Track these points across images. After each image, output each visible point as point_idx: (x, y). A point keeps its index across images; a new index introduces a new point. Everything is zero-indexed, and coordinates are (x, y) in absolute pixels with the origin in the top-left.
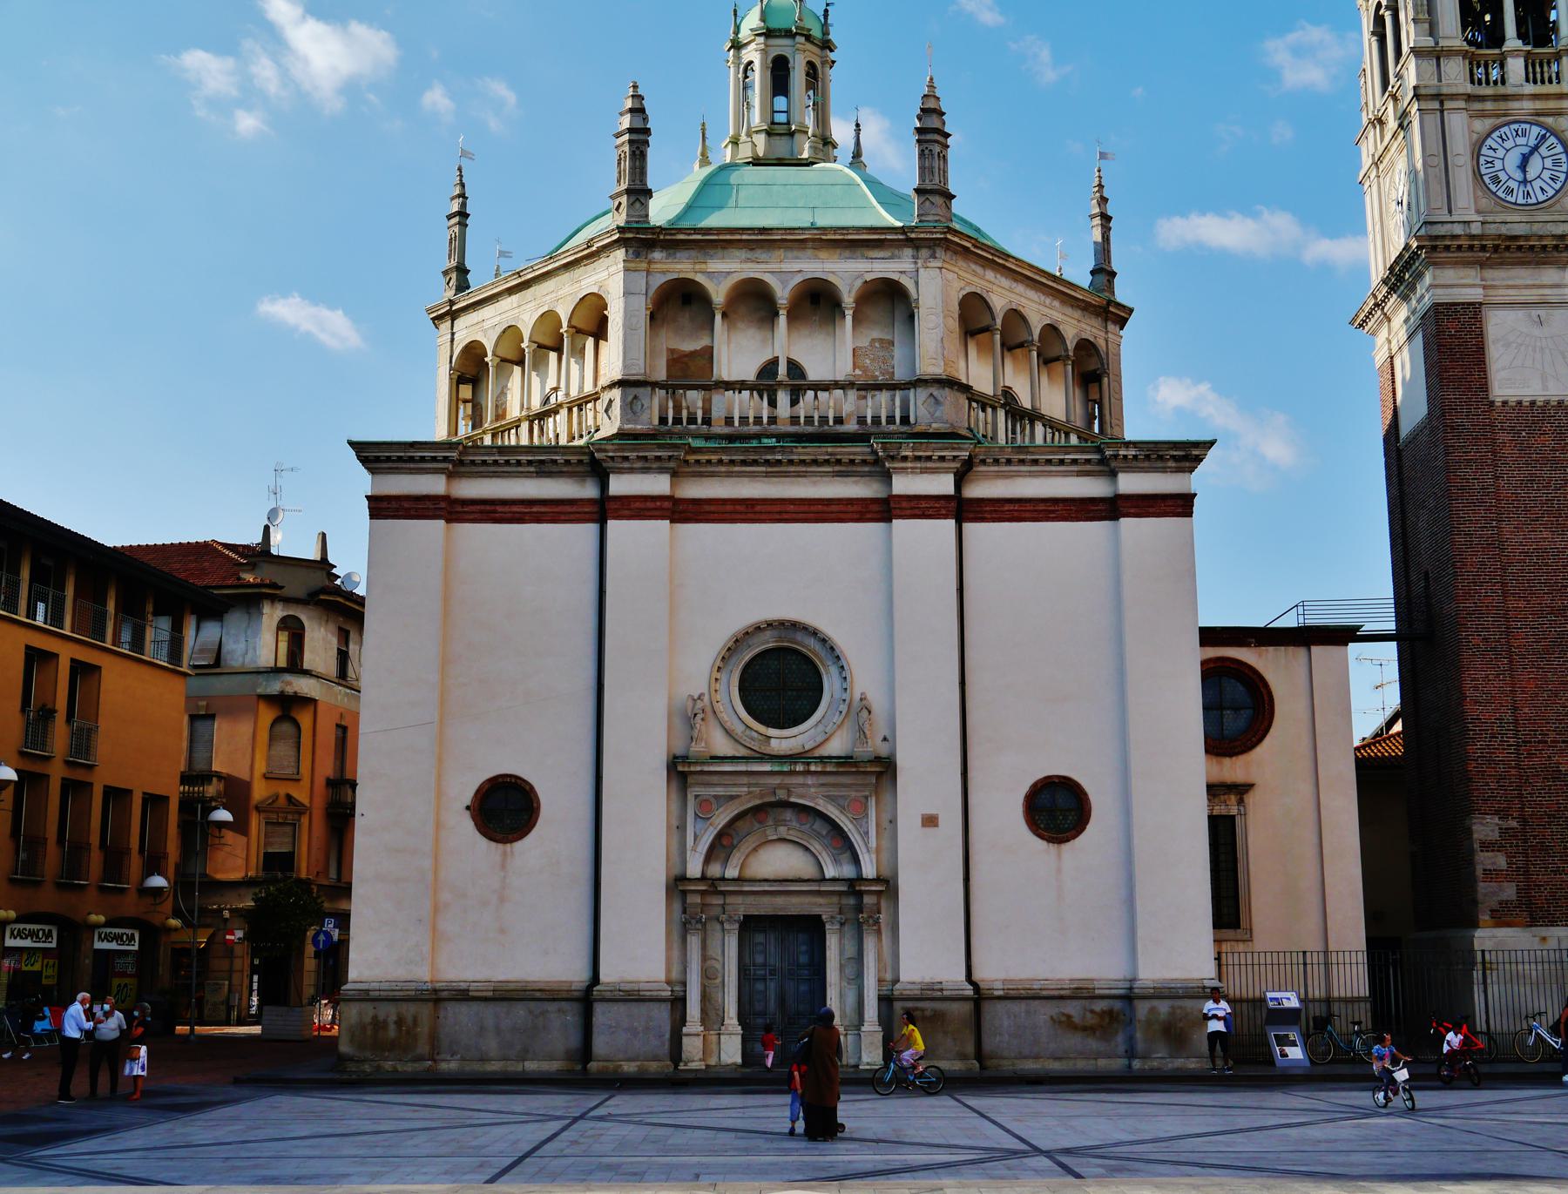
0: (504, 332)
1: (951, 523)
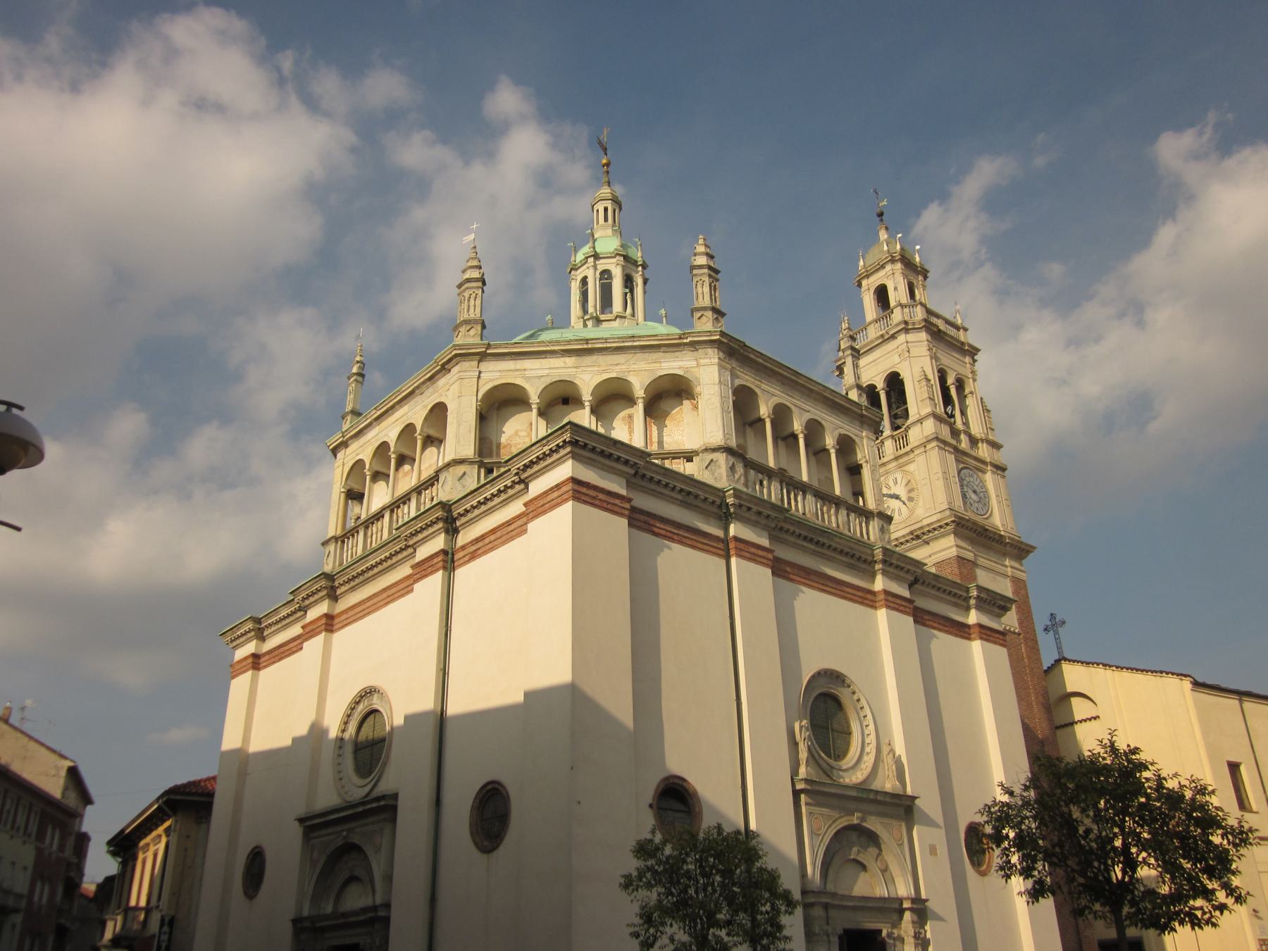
0: (552, 384)
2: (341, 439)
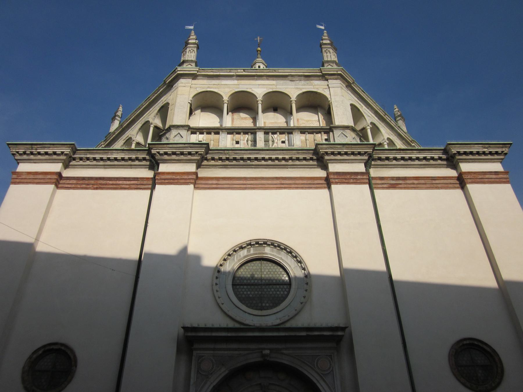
2: (196, 72)
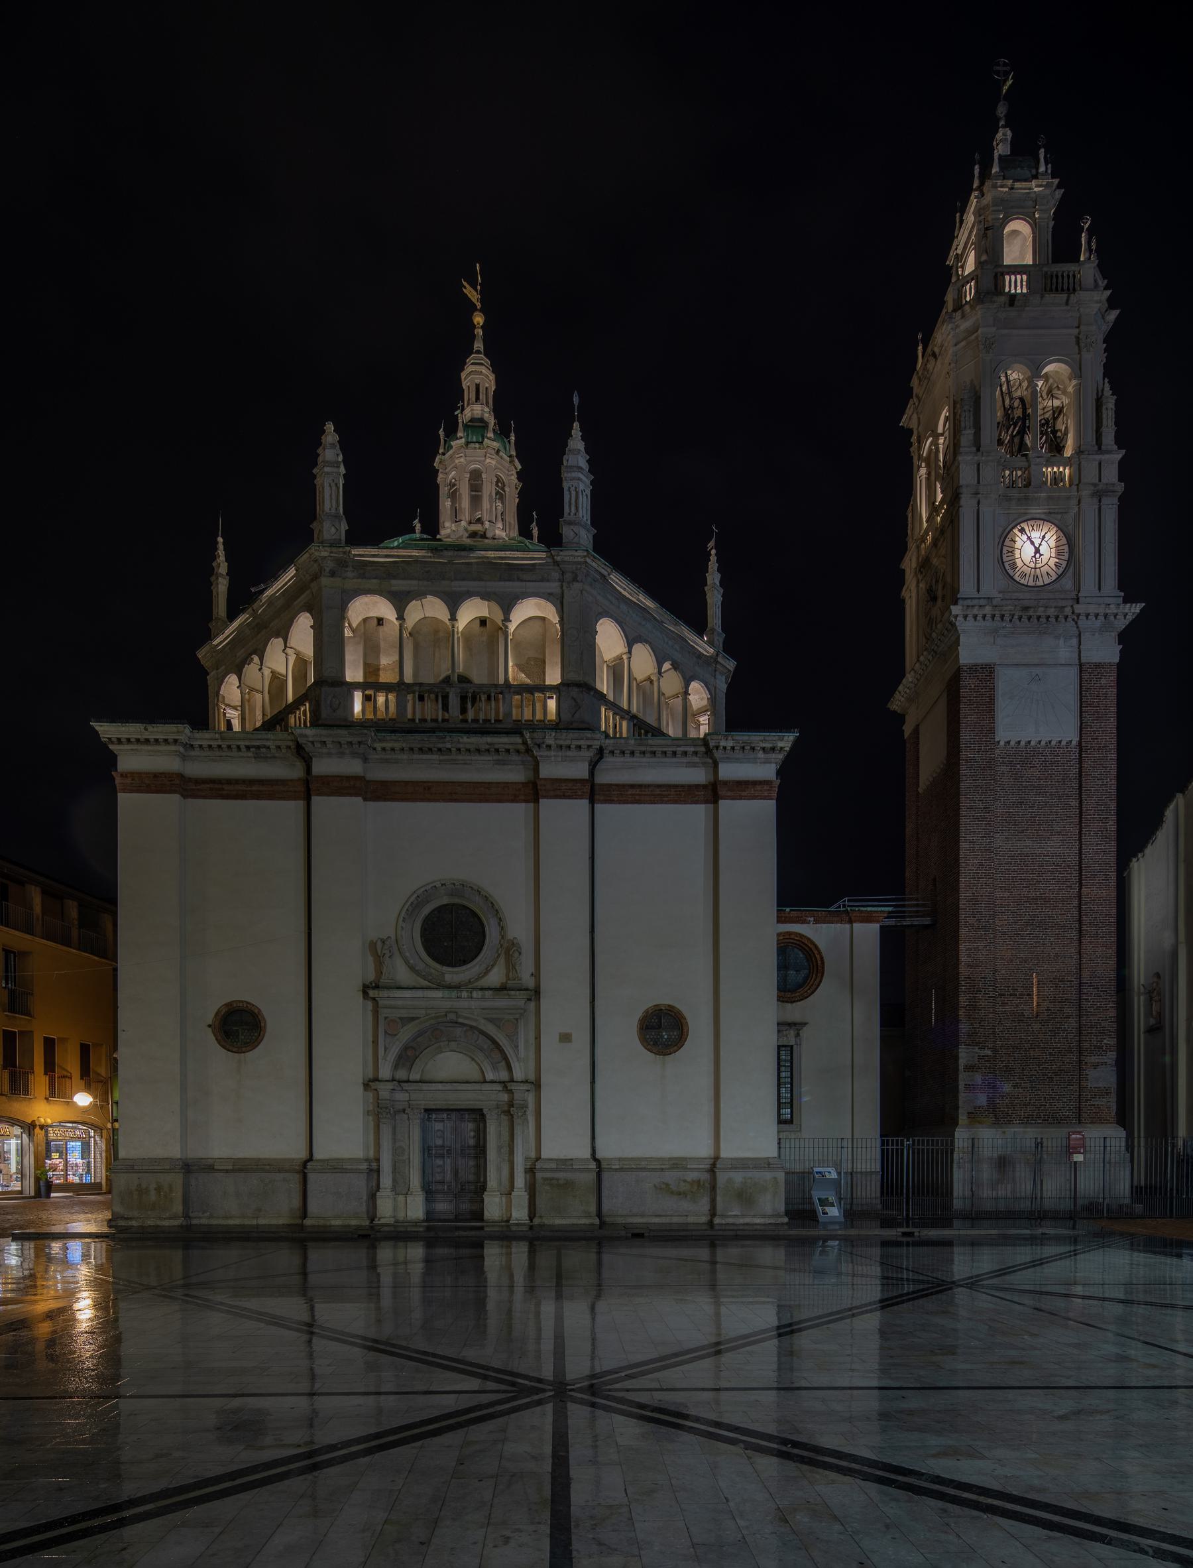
1: (585, 803)
